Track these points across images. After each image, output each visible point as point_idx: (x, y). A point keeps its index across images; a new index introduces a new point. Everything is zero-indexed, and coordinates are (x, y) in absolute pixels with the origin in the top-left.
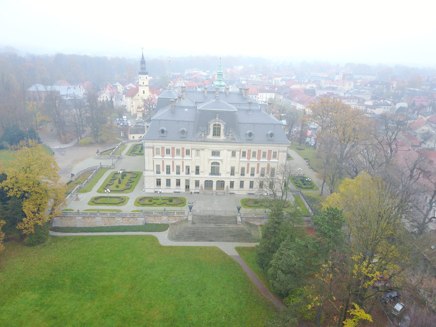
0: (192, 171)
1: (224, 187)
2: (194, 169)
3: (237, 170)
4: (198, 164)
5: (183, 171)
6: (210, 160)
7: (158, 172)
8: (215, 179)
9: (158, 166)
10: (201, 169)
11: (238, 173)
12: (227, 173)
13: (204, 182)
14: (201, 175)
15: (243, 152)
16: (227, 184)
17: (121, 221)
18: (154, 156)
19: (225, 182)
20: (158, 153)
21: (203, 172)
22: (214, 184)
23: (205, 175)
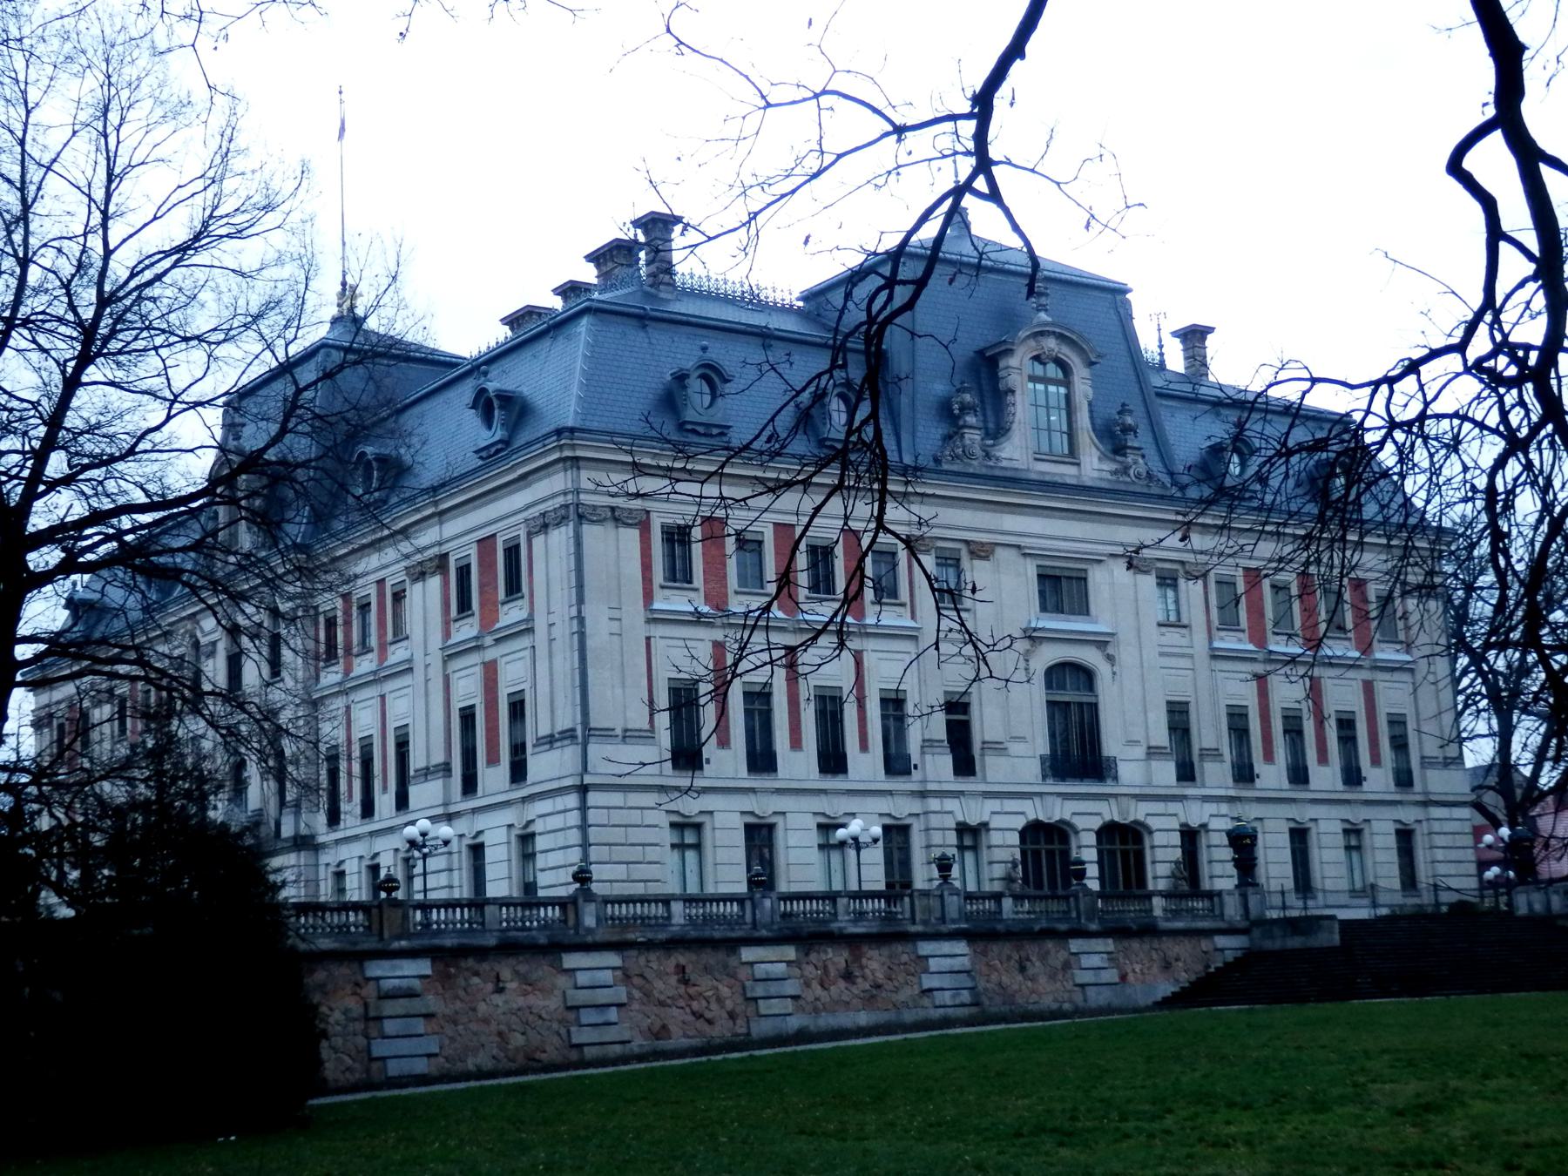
0: (928, 744)
2: (938, 726)
3: (1209, 732)
5: (864, 747)
6: (1033, 637)
7: (687, 756)
8: (1085, 812)
9: (683, 701)
10: (986, 723)
11: (1215, 754)
12: (1153, 752)
13: (1014, 839)
14: (994, 770)
17: (791, 988)
18: (648, 596)
20: (679, 574)
21: (997, 748)
23: (1015, 785)
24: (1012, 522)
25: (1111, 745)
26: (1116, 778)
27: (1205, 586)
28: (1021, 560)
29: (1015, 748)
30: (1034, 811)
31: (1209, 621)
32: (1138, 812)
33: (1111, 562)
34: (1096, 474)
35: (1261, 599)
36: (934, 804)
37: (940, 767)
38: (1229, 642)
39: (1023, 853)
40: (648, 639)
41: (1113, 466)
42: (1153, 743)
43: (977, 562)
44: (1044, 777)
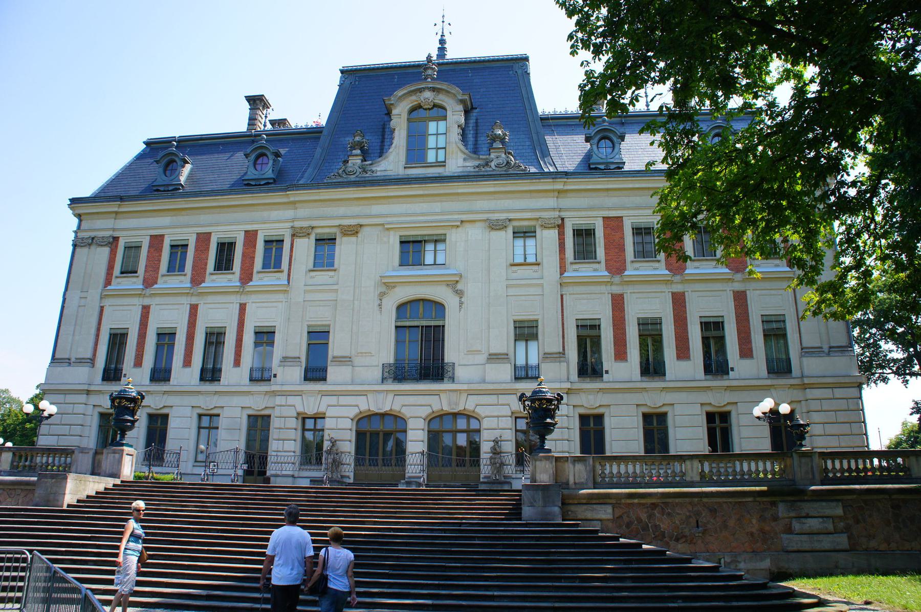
1: (476, 463)
4: (319, 317)
6: (388, 286)
8: (416, 405)
9: (118, 340)
10: (337, 346)
12: (494, 358)
13: (348, 424)
15: (578, 233)
16: (495, 434)
18: (108, 282)
19: (486, 424)
21: (345, 360)
22: (411, 435)
24: (377, 209)
25: (451, 354)
26: (452, 379)
27: (561, 235)
28: (387, 232)
29: (357, 361)
30: (366, 405)
31: (562, 259)
32: (469, 404)
33: (467, 225)
34: (460, 170)
35: (623, 238)
36: (279, 400)
37: (290, 376)
38: (586, 270)
39: (360, 435)
40: (102, 308)
41: (477, 163)
42: (491, 352)
43: (345, 239)
44: (383, 380)
